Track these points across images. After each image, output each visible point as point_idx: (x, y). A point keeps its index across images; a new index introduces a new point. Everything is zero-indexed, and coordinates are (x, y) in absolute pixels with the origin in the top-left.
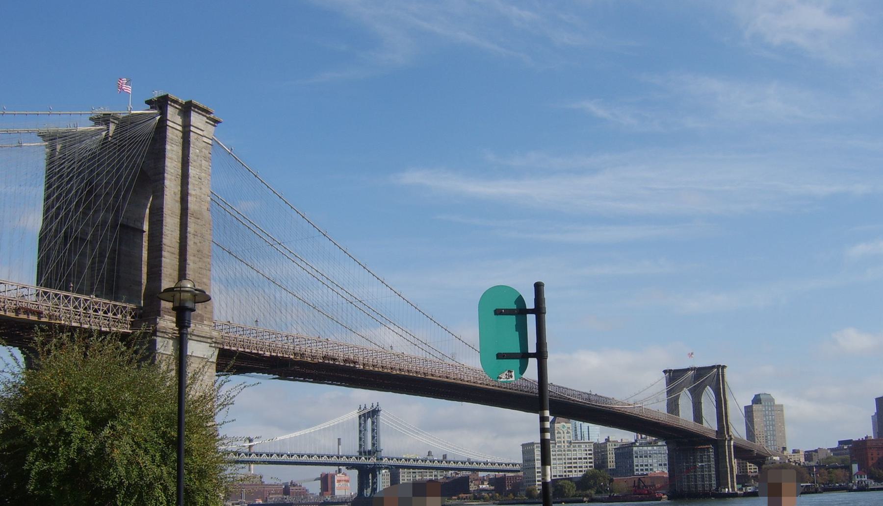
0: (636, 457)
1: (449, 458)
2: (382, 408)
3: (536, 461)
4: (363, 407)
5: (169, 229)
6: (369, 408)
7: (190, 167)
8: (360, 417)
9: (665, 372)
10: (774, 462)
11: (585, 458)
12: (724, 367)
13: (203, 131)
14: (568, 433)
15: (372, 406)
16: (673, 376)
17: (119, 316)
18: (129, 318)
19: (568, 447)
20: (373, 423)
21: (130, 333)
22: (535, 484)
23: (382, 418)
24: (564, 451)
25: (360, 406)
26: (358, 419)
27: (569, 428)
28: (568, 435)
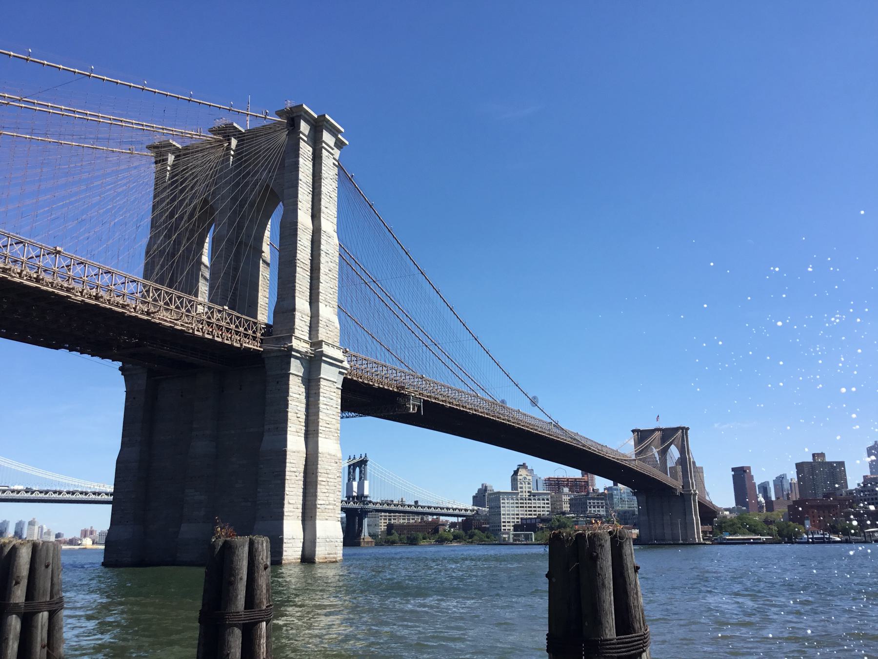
0: (590, 507)
1: (419, 504)
2: (369, 459)
3: (502, 509)
4: (352, 458)
5: (302, 244)
6: (358, 459)
7: (323, 184)
8: (349, 466)
9: (633, 431)
10: (725, 517)
11: (543, 507)
12: (687, 429)
13: (333, 149)
14: (529, 484)
15: (361, 457)
16: (642, 436)
17: (250, 332)
18: (259, 335)
19: (529, 496)
20: (361, 472)
21: (260, 351)
22: (501, 530)
23: (369, 467)
24: (526, 500)
25: (361, 455)
26: (348, 468)
27: (529, 480)
28: (529, 486)
